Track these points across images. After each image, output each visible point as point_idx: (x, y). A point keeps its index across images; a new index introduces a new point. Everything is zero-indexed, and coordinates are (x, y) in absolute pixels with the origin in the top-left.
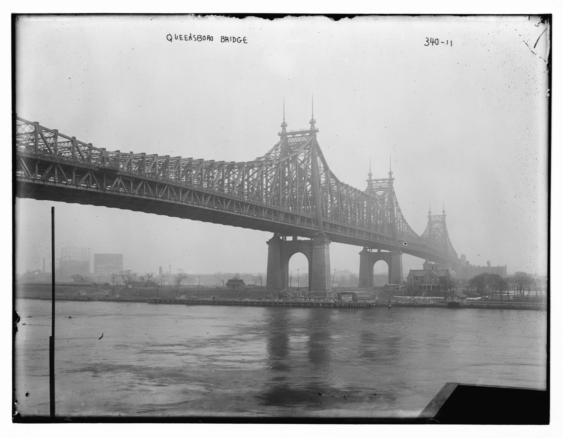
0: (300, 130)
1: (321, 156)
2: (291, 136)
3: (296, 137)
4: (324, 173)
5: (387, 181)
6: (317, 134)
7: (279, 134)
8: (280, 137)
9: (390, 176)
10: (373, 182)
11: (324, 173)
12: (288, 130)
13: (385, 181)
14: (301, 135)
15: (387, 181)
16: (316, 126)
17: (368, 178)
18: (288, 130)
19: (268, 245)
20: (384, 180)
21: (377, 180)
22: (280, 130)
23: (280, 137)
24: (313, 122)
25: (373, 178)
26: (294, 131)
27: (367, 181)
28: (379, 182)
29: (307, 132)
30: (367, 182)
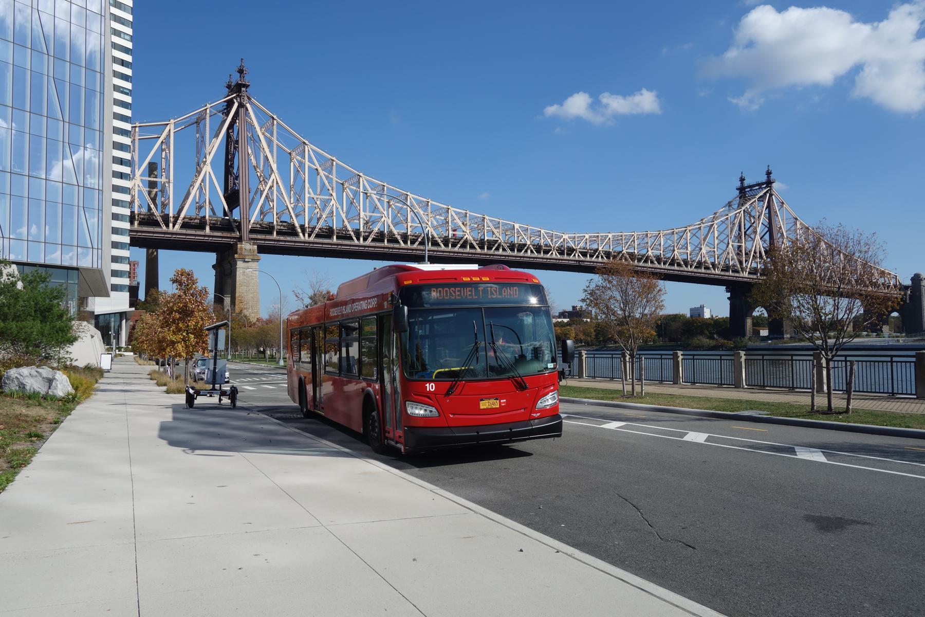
0: (755, 183)
2: (747, 190)
6: (774, 185)
14: (757, 187)
16: (772, 177)
24: (769, 173)
29: (763, 184)
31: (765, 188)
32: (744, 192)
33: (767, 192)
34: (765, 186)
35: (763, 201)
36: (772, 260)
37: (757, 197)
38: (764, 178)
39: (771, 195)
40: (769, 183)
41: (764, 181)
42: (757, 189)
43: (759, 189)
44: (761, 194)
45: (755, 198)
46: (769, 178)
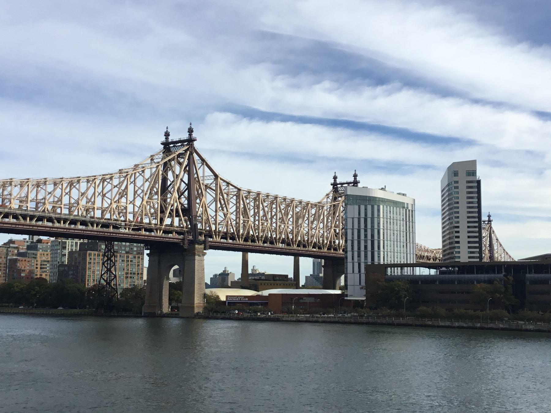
1: (205, 163)
2: (172, 145)
3: (177, 146)
4: (215, 182)
5: (353, 184)
6: (195, 142)
7: (162, 144)
8: (163, 146)
9: (354, 178)
10: (338, 186)
11: (215, 182)
12: (171, 139)
13: (351, 185)
14: (180, 144)
15: (353, 184)
16: (194, 135)
17: (332, 181)
18: (171, 139)
19: (148, 258)
20: (348, 183)
21: (342, 184)
22: (163, 139)
23: (163, 146)
25: (338, 181)
26: (174, 141)
27: (332, 185)
28: (344, 185)
30: (332, 186)
31: (187, 145)
32: (167, 147)
33: (188, 149)
34: (186, 143)
35: (183, 158)
36: (189, 217)
37: (177, 153)
38: (185, 136)
39: (191, 154)
40: (190, 141)
41: (186, 138)
42: (179, 146)
43: (181, 145)
44: (181, 151)
45: (175, 153)
46: (190, 137)
